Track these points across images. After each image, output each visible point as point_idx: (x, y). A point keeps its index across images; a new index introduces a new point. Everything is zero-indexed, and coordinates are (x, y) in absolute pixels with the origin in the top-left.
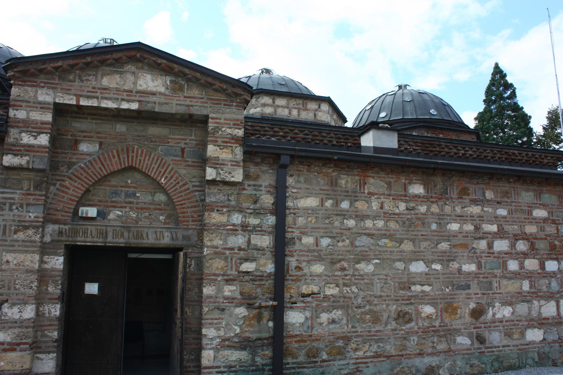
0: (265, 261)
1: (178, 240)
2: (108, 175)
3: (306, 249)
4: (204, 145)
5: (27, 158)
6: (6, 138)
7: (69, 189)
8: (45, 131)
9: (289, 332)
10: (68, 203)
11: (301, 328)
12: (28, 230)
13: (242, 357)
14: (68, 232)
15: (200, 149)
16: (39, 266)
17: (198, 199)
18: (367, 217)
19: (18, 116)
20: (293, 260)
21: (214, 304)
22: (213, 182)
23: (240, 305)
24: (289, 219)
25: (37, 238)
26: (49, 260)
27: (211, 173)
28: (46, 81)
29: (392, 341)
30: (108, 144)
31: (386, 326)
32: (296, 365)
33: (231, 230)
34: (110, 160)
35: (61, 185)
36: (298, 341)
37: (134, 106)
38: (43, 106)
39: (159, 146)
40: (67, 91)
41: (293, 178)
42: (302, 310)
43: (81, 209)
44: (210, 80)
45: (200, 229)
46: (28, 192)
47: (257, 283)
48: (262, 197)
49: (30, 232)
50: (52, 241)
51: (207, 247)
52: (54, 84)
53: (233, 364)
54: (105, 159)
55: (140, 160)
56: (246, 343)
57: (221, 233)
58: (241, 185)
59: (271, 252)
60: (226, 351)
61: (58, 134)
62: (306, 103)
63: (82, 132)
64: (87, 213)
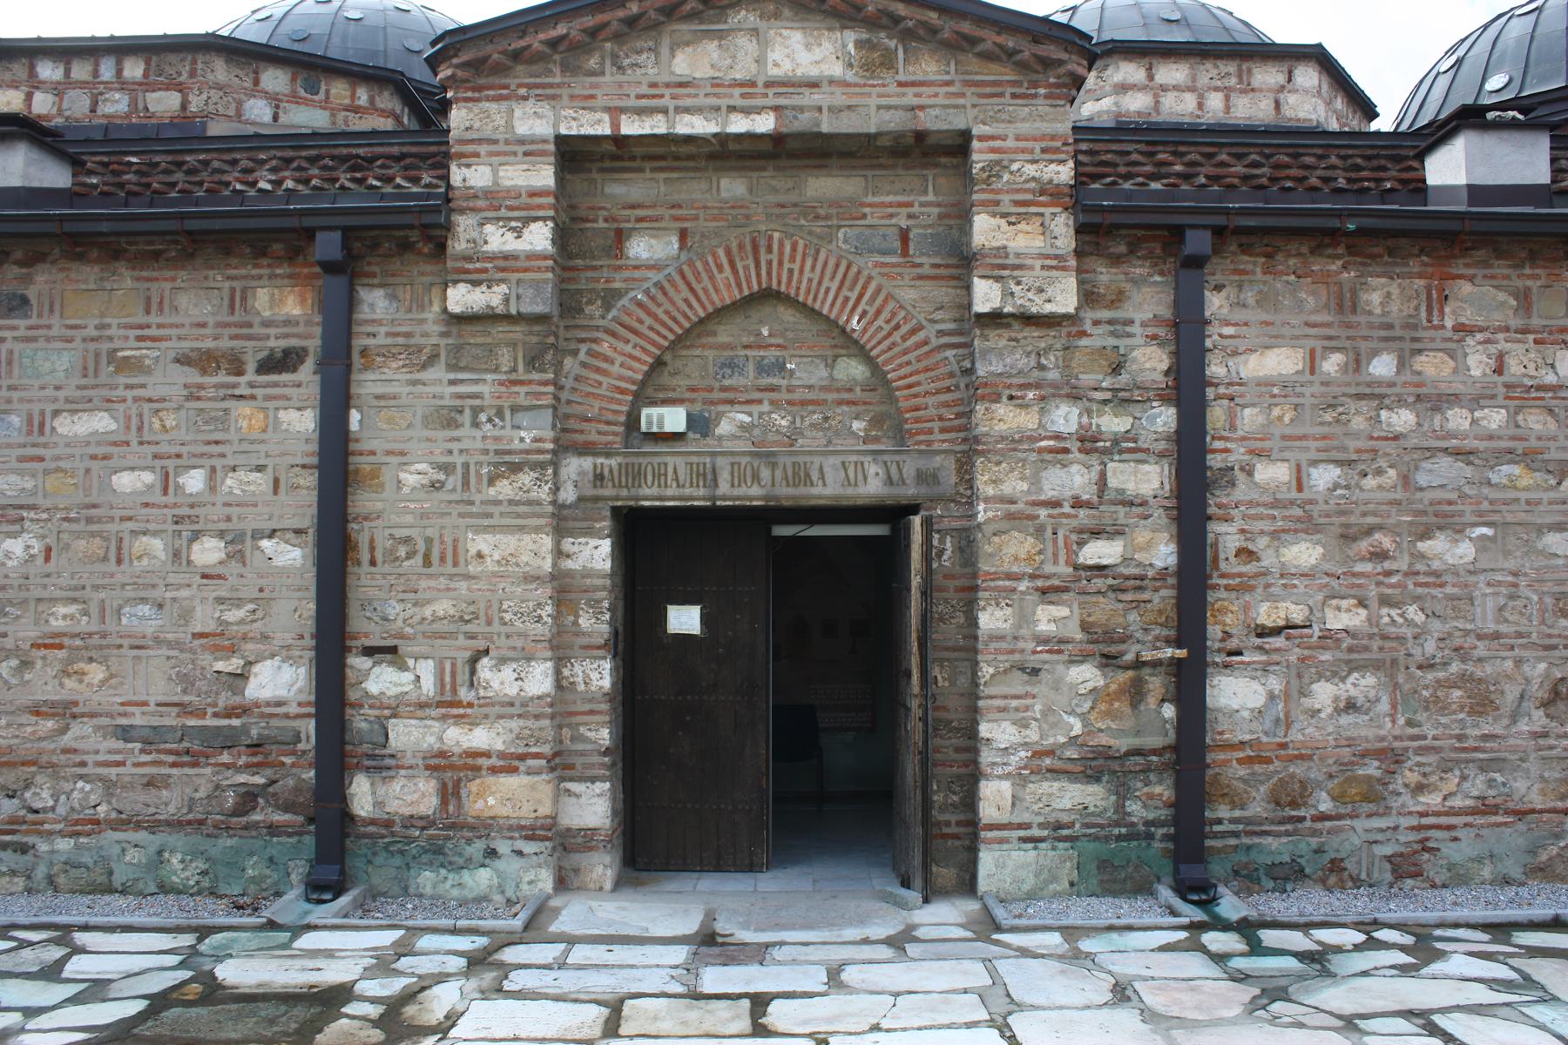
0: (1147, 535)
1: (904, 483)
2: (709, 317)
3: (1267, 499)
4: (962, 216)
5: (503, 288)
6: (450, 242)
7: (612, 363)
8: (541, 213)
9: (1221, 733)
10: (611, 400)
11: (1255, 725)
12: (521, 475)
13: (1088, 800)
14: (616, 473)
15: (951, 227)
16: (554, 565)
17: (955, 367)
18: (1454, 399)
19: (472, 183)
20: (1230, 530)
21: (1010, 657)
22: (995, 319)
23: (1082, 658)
24: (1217, 415)
25: (544, 493)
26: (576, 548)
27: (986, 295)
28: (532, 80)
29: (1533, 766)
30: (703, 235)
31: (1514, 722)
32: (1241, 827)
33: (1051, 450)
34: (712, 278)
35: (590, 353)
36: (1249, 760)
37: (764, 124)
38: (528, 149)
39: (839, 227)
40: (585, 102)
41: (1224, 293)
42: (1259, 673)
43: (645, 412)
44: (966, 27)
45: (963, 452)
46: (513, 376)
47: (1129, 597)
48: (1135, 354)
49: (526, 478)
50: (581, 499)
51: (987, 500)
52: (551, 86)
53: (1065, 818)
54: (697, 275)
55: (791, 271)
56: (1101, 762)
57: (1024, 460)
58: (1073, 324)
59: (1166, 508)
60: (1046, 785)
61: (573, 219)
62: (1249, 71)
63: (633, 207)
64: (661, 423)
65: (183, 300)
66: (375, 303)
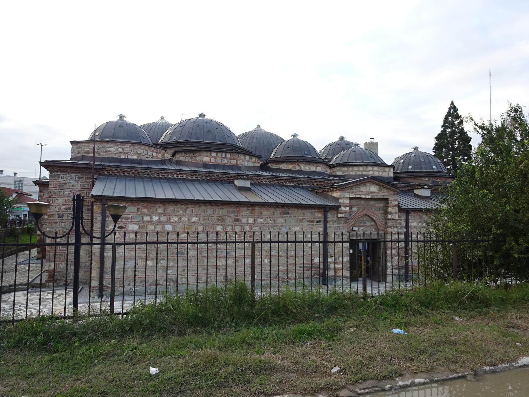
22: (390, 219)
27: (389, 217)
37: (370, 197)
38: (346, 198)
65: (307, 214)
66: (329, 215)
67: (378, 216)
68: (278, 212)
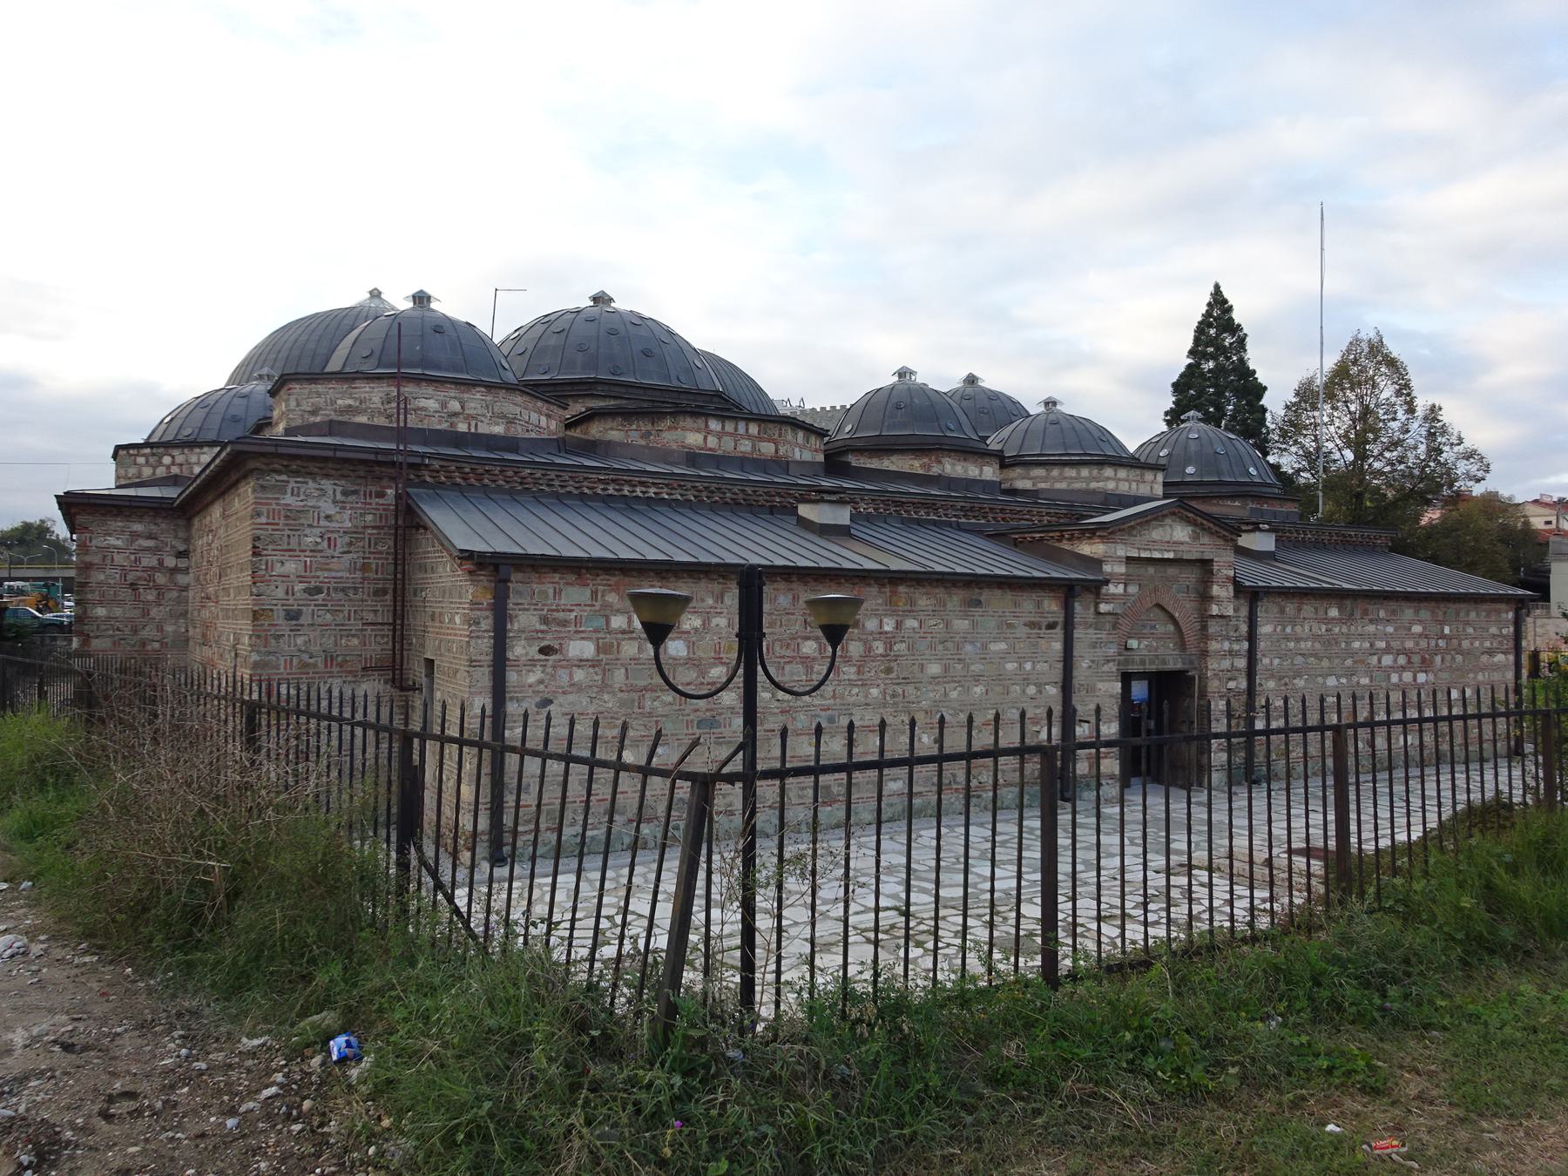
18: (1302, 639)
27: (1215, 610)
37: (1171, 555)
38: (1118, 560)
49: (1111, 664)
65: (1025, 604)
67: (1185, 609)
68: (955, 600)
